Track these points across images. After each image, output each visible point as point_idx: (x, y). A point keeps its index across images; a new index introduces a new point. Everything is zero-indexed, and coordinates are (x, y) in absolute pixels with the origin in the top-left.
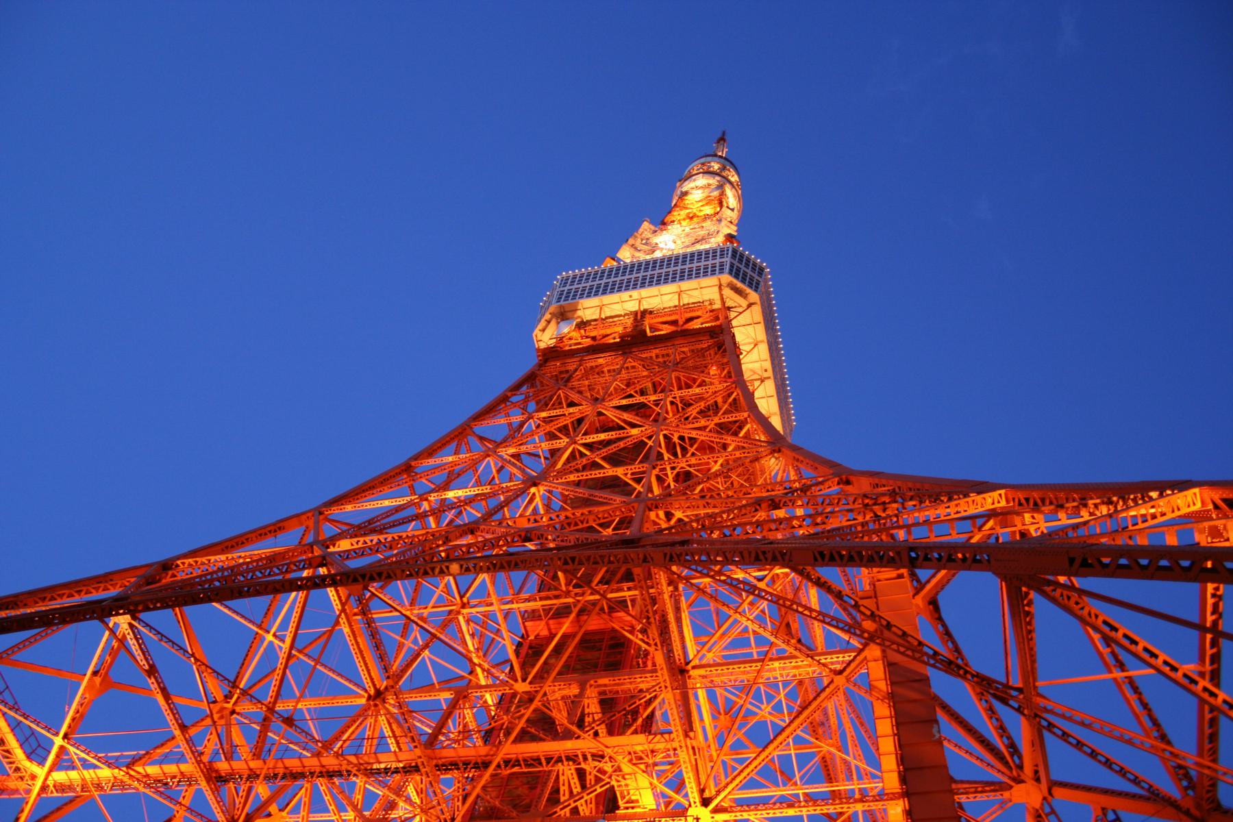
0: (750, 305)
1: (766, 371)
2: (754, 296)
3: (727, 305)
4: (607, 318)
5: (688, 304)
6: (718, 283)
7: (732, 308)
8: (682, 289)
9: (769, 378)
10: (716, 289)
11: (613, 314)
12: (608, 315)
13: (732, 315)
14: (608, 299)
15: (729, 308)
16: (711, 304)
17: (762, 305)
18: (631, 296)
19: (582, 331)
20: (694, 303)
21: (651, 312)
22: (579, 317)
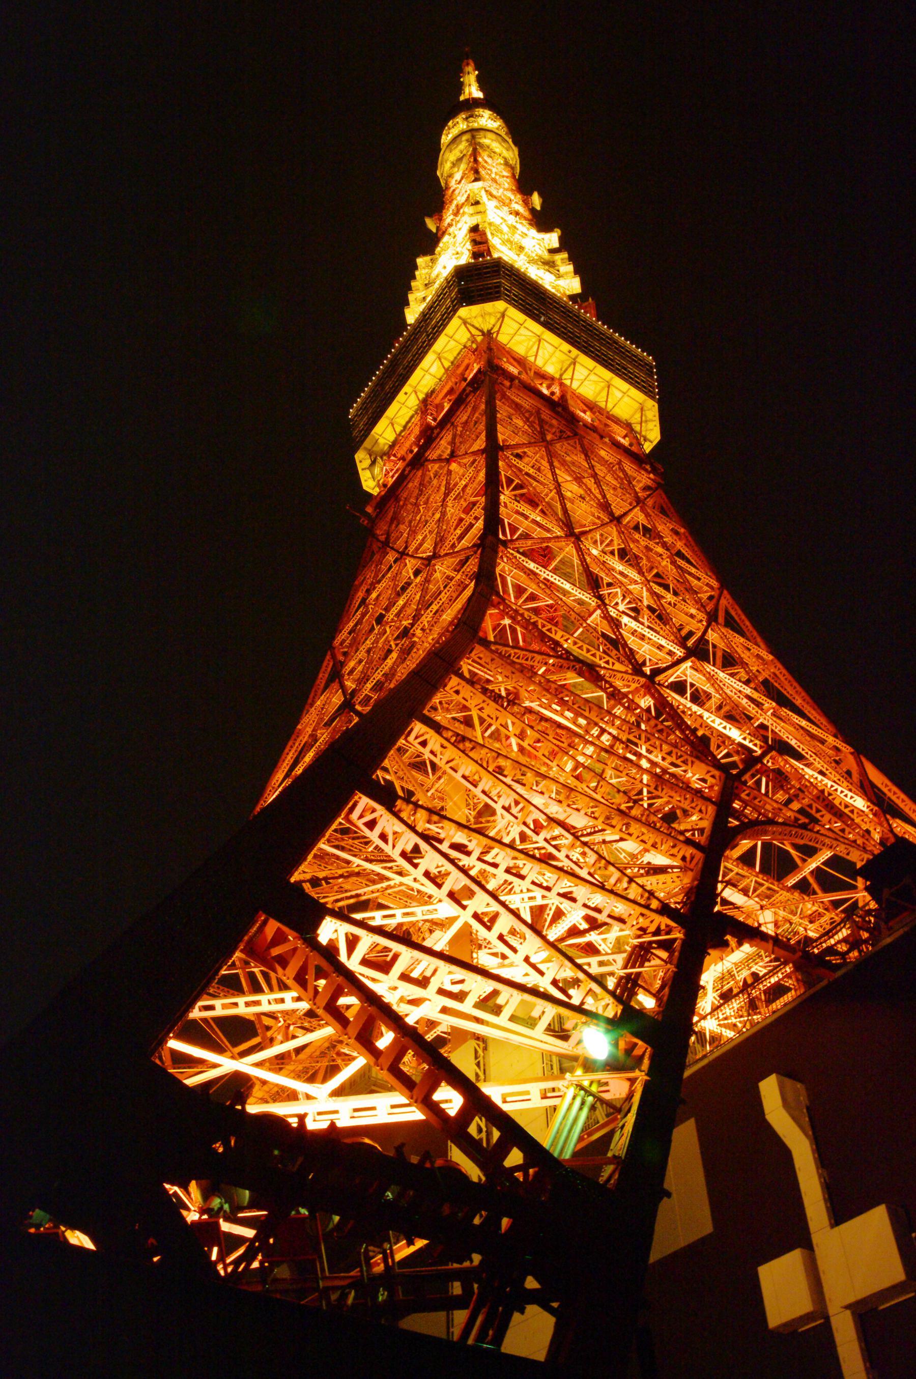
0: (503, 315)
1: (570, 352)
2: (501, 305)
3: (485, 331)
4: (405, 427)
5: (455, 358)
6: (460, 322)
7: (492, 329)
8: (439, 352)
9: (577, 356)
10: (463, 326)
11: (407, 419)
12: (404, 423)
13: (495, 335)
14: (391, 411)
15: (489, 333)
16: (473, 342)
17: (514, 306)
18: (406, 393)
19: (392, 458)
20: (459, 354)
21: (433, 392)
22: (385, 444)
